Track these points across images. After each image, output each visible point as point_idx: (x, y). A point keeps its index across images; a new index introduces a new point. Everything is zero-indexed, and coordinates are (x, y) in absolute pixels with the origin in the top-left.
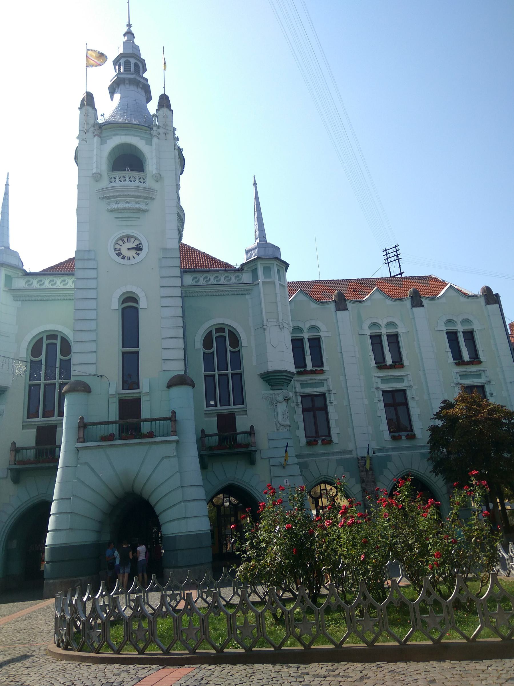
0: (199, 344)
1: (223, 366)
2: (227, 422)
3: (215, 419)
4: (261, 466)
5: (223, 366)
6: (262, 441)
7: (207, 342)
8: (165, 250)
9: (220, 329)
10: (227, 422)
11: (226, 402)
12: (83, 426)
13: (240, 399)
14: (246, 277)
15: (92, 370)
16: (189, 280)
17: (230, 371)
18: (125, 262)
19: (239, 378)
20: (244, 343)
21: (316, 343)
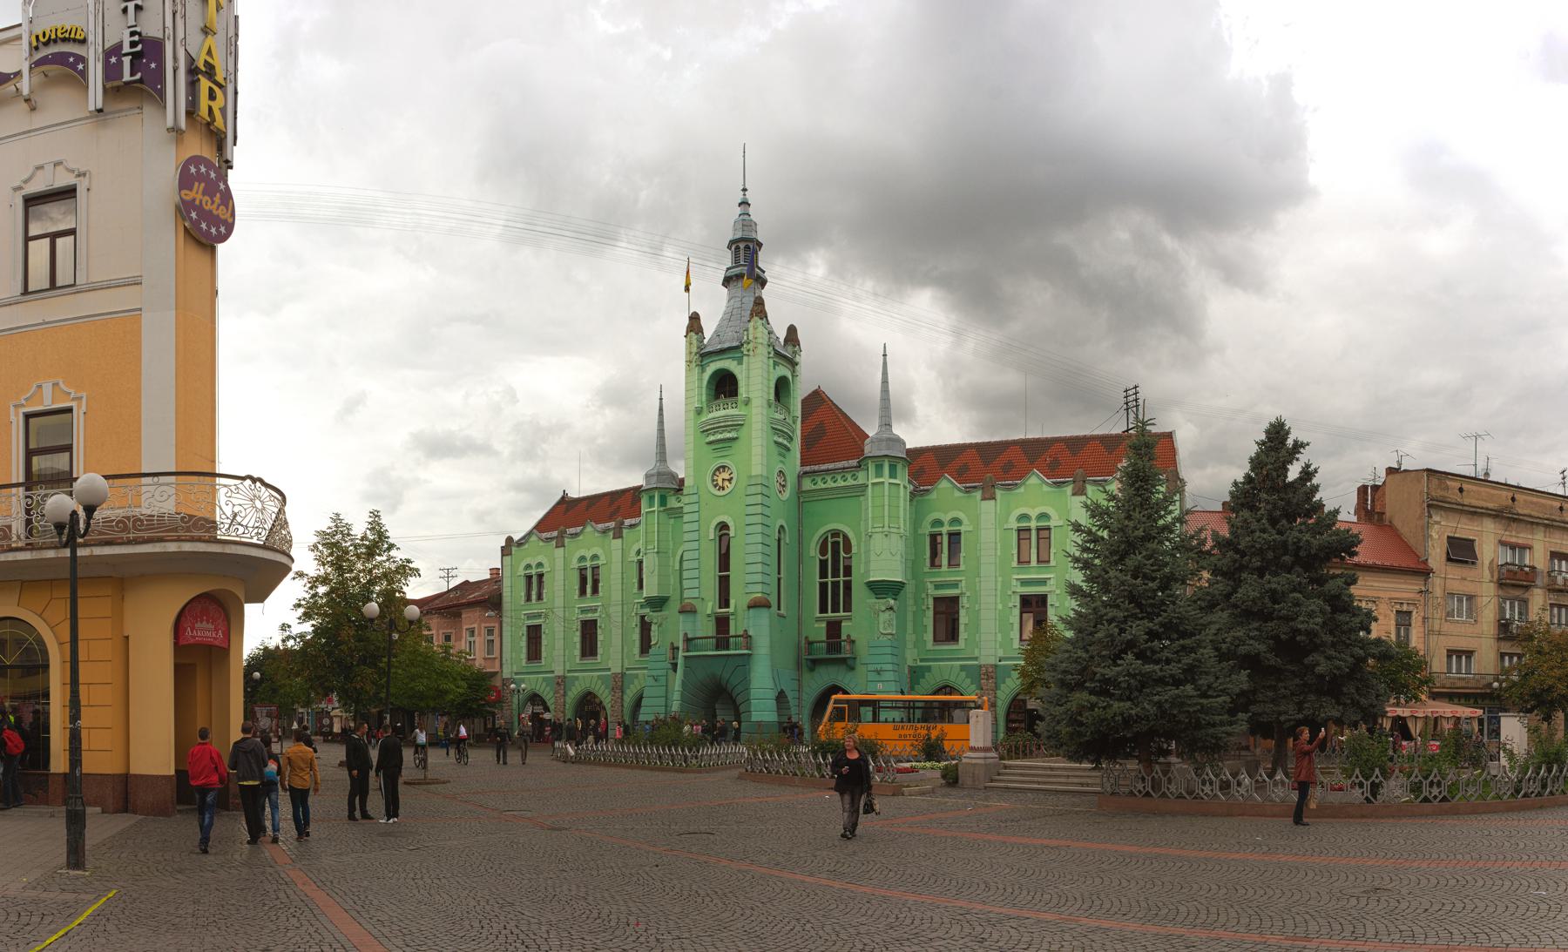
0: (813, 551)
1: (836, 574)
2: (834, 628)
3: (824, 625)
4: (861, 670)
5: (836, 574)
6: (862, 648)
7: (823, 551)
8: (750, 477)
9: (836, 534)
10: (834, 628)
11: (836, 610)
12: (688, 640)
13: (848, 608)
14: (861, 475)
15: (695, 593)
16: (807, 484)
17: (842, 578)
18: (722, 493)
19: (848, 586)
20: (854, 550)
21: (955, 537)
